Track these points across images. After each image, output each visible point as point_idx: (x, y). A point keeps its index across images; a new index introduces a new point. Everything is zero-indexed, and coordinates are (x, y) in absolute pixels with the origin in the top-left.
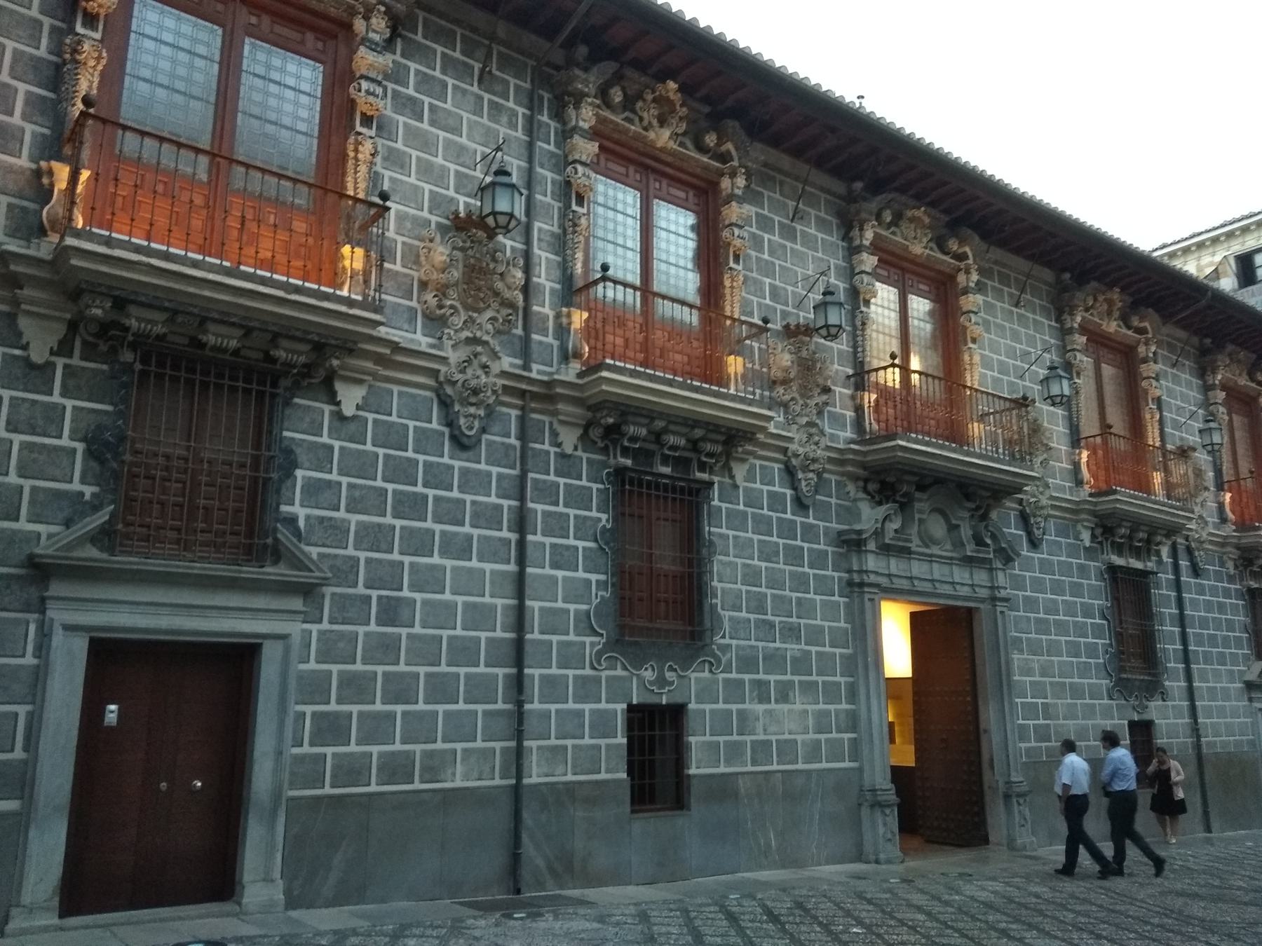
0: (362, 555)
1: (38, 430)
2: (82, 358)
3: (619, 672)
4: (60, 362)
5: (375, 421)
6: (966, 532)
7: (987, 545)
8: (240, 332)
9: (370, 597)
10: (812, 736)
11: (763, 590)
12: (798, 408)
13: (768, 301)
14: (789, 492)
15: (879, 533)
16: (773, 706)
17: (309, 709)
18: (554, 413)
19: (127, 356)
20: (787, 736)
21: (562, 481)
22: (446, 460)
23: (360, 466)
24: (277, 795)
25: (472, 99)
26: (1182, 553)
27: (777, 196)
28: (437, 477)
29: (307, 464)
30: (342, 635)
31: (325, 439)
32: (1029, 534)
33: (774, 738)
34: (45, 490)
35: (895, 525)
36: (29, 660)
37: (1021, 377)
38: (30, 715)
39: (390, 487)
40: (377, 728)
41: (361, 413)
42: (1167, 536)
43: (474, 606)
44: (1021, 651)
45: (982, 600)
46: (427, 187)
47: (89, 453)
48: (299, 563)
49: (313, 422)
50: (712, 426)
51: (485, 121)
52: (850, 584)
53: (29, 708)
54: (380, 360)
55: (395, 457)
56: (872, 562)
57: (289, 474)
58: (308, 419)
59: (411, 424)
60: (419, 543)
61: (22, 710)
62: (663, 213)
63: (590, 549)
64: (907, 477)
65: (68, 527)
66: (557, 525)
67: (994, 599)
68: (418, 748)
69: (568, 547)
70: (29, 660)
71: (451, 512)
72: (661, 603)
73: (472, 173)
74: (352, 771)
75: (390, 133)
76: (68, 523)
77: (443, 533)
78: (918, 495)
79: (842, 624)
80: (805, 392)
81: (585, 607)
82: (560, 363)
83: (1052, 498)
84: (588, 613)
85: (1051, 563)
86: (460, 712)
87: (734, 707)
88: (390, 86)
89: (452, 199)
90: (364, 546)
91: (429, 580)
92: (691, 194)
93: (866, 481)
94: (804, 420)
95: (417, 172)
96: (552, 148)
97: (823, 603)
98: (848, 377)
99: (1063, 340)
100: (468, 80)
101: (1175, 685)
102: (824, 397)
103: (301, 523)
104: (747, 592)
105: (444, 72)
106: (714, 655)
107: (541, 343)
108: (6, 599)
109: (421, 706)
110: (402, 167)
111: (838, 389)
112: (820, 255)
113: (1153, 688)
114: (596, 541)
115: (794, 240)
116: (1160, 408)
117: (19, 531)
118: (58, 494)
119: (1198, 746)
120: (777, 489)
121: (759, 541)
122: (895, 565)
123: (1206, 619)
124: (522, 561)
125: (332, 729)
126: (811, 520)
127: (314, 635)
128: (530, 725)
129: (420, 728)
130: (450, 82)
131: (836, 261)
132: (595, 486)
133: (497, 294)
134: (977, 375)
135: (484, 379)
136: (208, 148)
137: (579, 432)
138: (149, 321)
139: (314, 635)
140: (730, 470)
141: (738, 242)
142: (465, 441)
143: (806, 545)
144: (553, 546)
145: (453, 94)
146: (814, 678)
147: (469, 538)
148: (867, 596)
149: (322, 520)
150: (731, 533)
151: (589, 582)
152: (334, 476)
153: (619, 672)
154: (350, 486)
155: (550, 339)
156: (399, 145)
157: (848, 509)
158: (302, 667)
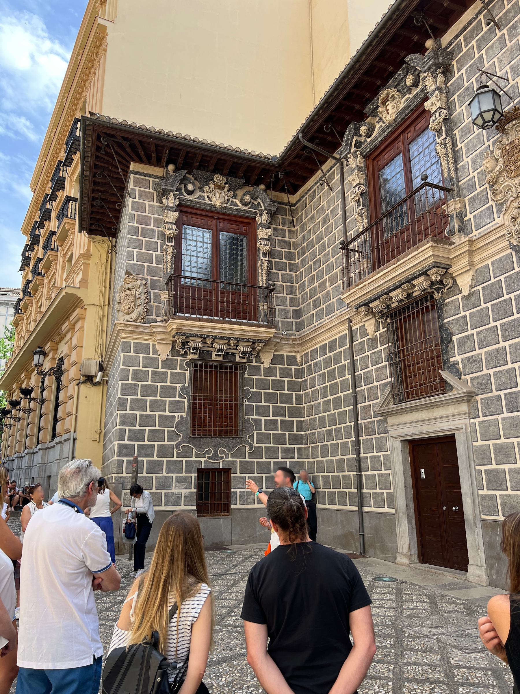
0: (491, 371)
29: (457, 332)
57: (451, 341)
58: (453, 308)
90: (491, 366)
127: (477, 424)
139: (477, 424)
149: (468, 359)
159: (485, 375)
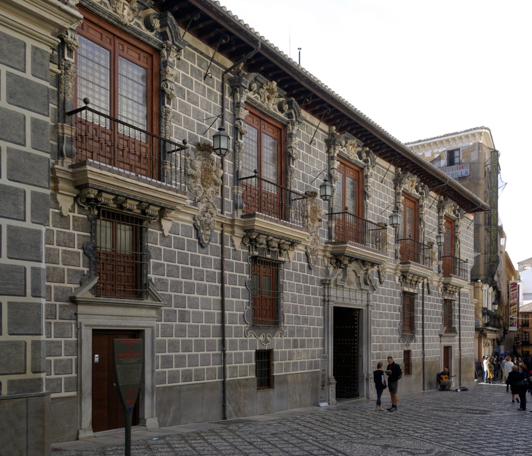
0: (173, 294)
1: (67, 245)
2: (79, 213)
5: (174, 237)
7: (368, 285)
9: (176, 311)
10: (310, 360)
11: (297, 304)
13: (301, 181)
14: (306, 264)
16: (299, 349)
17: (160, 354)
20: (303, 360)
22: (197, 254)
23: (170, 257)
24: (153, 387)
25: (201, 87)
26: (426, 286)
27: (305, 132)
29: (153, 257)
31: (159, 246)
32: (380, 279)
36: (74, 339)
39: (180, 265)
40: (181, 361)
41: (170, 234)
44: (374, 325)
47: (84, 253)
49: (154, 239)
51: (206, 98)
53: (76, 357)
58: (153, 238)
59: (186, 238)
60: (190, 289)
61: (74, 358)
62: (265, 140)
63: (244, 289)
64: (346, 258)
65: (81, 285)
69: (237, 289)
73: (202, 123)
74: (174, 377)
78: (349, 265)
80: (313, 221)
82: (234, 210)
85: (385, 290)
89: (196, 136)
90: (173, 290)
91: (194, 304)
93: (331, 258)
95: (184, 124)
97: (316, 309)
98: (327, 214)
99: (396, 197)
100: (200, 79)
101: (419, 337)
102: (320, 223)
103: (153, 281)
104: (292, 305)
107: (227, 201)
108: (64, 315)
111: (323, 219)
112: (319, 160)
113: (412, 338)
114: (246, 286)
115: (310, 153)
118: (76, 272)
119: (423, 359)
120: (302, 263)
121: (297, 284)
122: (339, 293)
123: (430, 311)
124: (223, 295)
125: (167, 362)
126: (313, 275)
129: (193, 361)
131: (324, 163)
137: (241, 240)
141: (294, 156)
142: (204, 245)
143: (311, 286)
144: (232, 288)
145: (195, 86)
146: (311, 338)
147: (206, 286)
149: (159, 279)
151: (243, 302)
152: (162, 262)
153: (253, 338)
154: (168, 265)
158: (157, 338)
159: (169, 295)
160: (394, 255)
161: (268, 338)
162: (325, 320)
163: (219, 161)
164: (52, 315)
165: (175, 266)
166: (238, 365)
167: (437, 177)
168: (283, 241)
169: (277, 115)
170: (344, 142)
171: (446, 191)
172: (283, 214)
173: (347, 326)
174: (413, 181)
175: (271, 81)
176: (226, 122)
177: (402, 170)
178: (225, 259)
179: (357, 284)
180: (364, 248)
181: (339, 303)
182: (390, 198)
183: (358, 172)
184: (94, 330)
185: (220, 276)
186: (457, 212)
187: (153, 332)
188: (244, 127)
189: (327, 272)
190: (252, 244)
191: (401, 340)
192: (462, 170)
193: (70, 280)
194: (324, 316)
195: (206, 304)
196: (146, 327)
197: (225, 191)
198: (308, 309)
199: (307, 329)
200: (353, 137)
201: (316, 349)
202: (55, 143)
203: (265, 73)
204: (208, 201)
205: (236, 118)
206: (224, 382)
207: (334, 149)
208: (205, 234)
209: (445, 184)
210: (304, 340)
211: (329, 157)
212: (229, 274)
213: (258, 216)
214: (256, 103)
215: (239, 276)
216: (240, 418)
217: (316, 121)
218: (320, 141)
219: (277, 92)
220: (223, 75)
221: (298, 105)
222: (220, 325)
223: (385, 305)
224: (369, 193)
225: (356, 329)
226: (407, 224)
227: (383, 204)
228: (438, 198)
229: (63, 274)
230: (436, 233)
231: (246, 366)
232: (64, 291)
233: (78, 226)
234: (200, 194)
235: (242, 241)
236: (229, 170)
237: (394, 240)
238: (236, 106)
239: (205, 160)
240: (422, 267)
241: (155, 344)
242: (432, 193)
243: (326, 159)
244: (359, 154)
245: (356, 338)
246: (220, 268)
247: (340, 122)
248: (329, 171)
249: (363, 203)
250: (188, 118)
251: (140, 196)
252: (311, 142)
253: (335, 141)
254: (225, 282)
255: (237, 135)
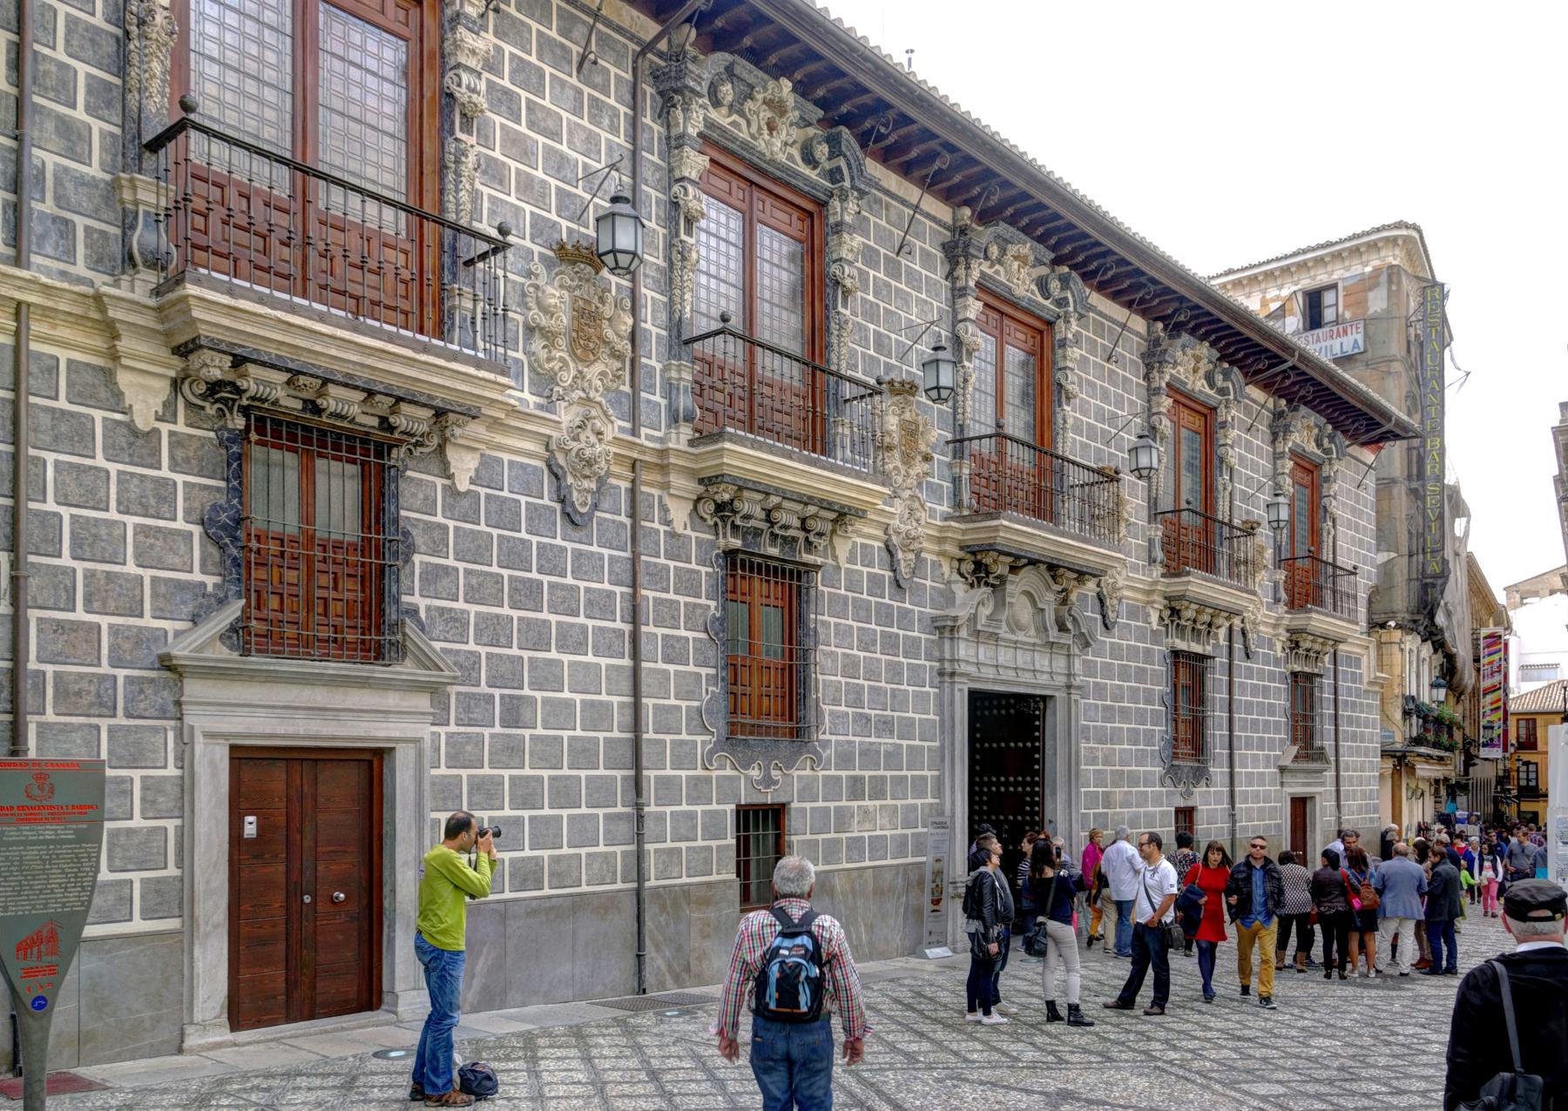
0: (483, 650)
1: (151, 511)
3: (729, 772)
4: (165, 428)
6: (1050, 617)
8: (362, 396)
9: (492, 696)
10: (899, 831)
11: (861, 681)
12: (900, 479)
13: (872, 352)
14: (888, 574)
15: (974, 618)
16: (867, 803)
18: (665, 486)
19: (239, 422)
20: (878, 833)
21: (672, 564)
22: (559, 541)
23: (475, 549)
26: (1237, 637)
27: (883, 223)
28: (551, 561)
29: (423, 548)
30: (468, 736)
33: (866, 835)
34: (167, 581)
35: (986, 611)
36: (172, 771)
37: (1108, 443)
38: (180, 831)
41: (473, 487)
42: (1228, 618)
43: (592, 703)
44: (1088, 740)
45: (1058, 689)
46: (528, 208)
48: (426, 661)
49: (426, 498)
50: (826, 505)
52: (941, 673)
53: (178, 822)
54: (495, 424)
55: (508, 539)
56: (964, 650)
57: (408, 560)
58: (421, 496)
59: (523, 499)
61: (171, 825)
62: (767, 242)
63: (700, 640)
64: (1002, 558)
65: (195, 623)
66: (667, 615)
67: (1069, 687)
68: (546, 854)
69: (679, 639)
70: (172, 771)
71: (566, 601)
72: (769, 697)
75: (487, 137)
76: (195, 620)
77: (558, 623)
78: (1011, 577)
79: (932, 717)
80: (907, 459)
81: (696, 704)
82: (669, 427)
83: (1128, 578)
84: (699, 710)
85: (1120, 646)
86: (583, 816)
87: (832, 805)
88: (485, 75)
90: (485, 640)
91: (548, 676)
92: (794, 217)
93: (960, 560)
94: (908, 492)
96: (655, 159)
97: (916, 695)
99: (1149, 401)
101: (1218, 771)
102: (926, 467)
103: (423, 615)
105: (540, 58)
106: (816, 753)
107: (648, 401)
108: (142, 705)
109: (547, 811)
110: (501, 182)
113: (1200, 775)
115: (898, 277)
116: (1231, 479)
117: (146, 628)
118: (181, 586)
120: (876, 570)
121: (859, 629)
122: (984, 653)
123: (1251, 703)
124: (635, 655)
126: (907, 605)
127: (443, 737)
128: (649, 825)
130: (548, 70)
131: (939, 305)
132: (703, 570)
133: (607, 343)
134: (1071, 443)
135: (599, 448)
136: (288, 155)
138: (268, 384)
139: (443, 737)
140: (833, 548)
141: (848, 282)
142: (577, 519)
143: (901, 632)
144: (665, 637)
146: (904, 773)
147: (584, 629)
148: (957, 687)
149: (442, 611)
150: (833, 620)
153: (729, 772)
154: (468, 572)
155: (657, 398)
156: (497, 154)
157: (941, 593)
158: (434, 772)
159: (471, 652)
160: (1145, 555)
161: (773, 773)
162: (947, 726)
163: (626, 294)
164: (101, 705)
165: (491, 574)
166: (683, 845)
167: (1267, 344)
168: (812, 509)
169: (797, 174)
170: (994, 251)
171: (1294, 384)
172: (815, 438)
173: (1007, 743)
174: (1198, 359)
175: (777, 79)
176: (644, 187)
177: (1165, 328)
178: (643, 558)
179: (1037, 630)
180: (1051, 531)
181: (987, 680)
182: (1131, 403)
183: (1041, 332)
184: (233, 748)
185: (628, 605)
186: (1326, 441)
187: (420, 754)
188: (694, 199)
189: (950, 598)
190: (722, 518)
191: (1168, 781)
192: (1344, 340)
193: (162, 610)
194: (941, 713)
195: (586, 678)
196: (398, 740)
197: (641, 374)
198: (894, 696)
199: (890, 749)
200: (1022, 235)
201: (919, 802)
202: (115, 231)
203: (756, 56)
204: (588, 399)
205: (673, 178)
206: (638, 892)
207: (968, 268)
208: (580, 490)
209: (1289, 364)
210: (883, 778)
211: (953, 289)
212: (655, 599)
213: (733, 439)
214: (734, 139)
215: (686, 604)
216: (686, 991)
217: (912, 192)
218: (927, 246)
219: (794, 108)
220: (635, 61)
221: (856, 146)
222: (629, 735)
223: (1121, 687)
224: (1070, 387)
225: (1037, 750)
226: (1183, 472)
227: (1114, 416)
228: (1270, 404)
229: (137, 592)
230: (1265, 497)
231: (709, 849)
232: (142, 638)
233: (187, 460)
234: (567, 377)
235: (695, 508)
236: (654, 318)
237: (1145, 514)
238: (674, 143)
239: (580, 287)
240: (1223, 584)
241: (427, 787)
242: (1255, 393)
243: (944, 294)
244: (1042, 285)
245: (1037, 773)
246: (629, 581)
247: (980, 195)
248: (954, 326)
249: (1053, 413)
250: (529, 175)
251: (366, 375)
252: (901, 247)
253: (967, 246)
254: (643, 619)
255: (677, 224)
